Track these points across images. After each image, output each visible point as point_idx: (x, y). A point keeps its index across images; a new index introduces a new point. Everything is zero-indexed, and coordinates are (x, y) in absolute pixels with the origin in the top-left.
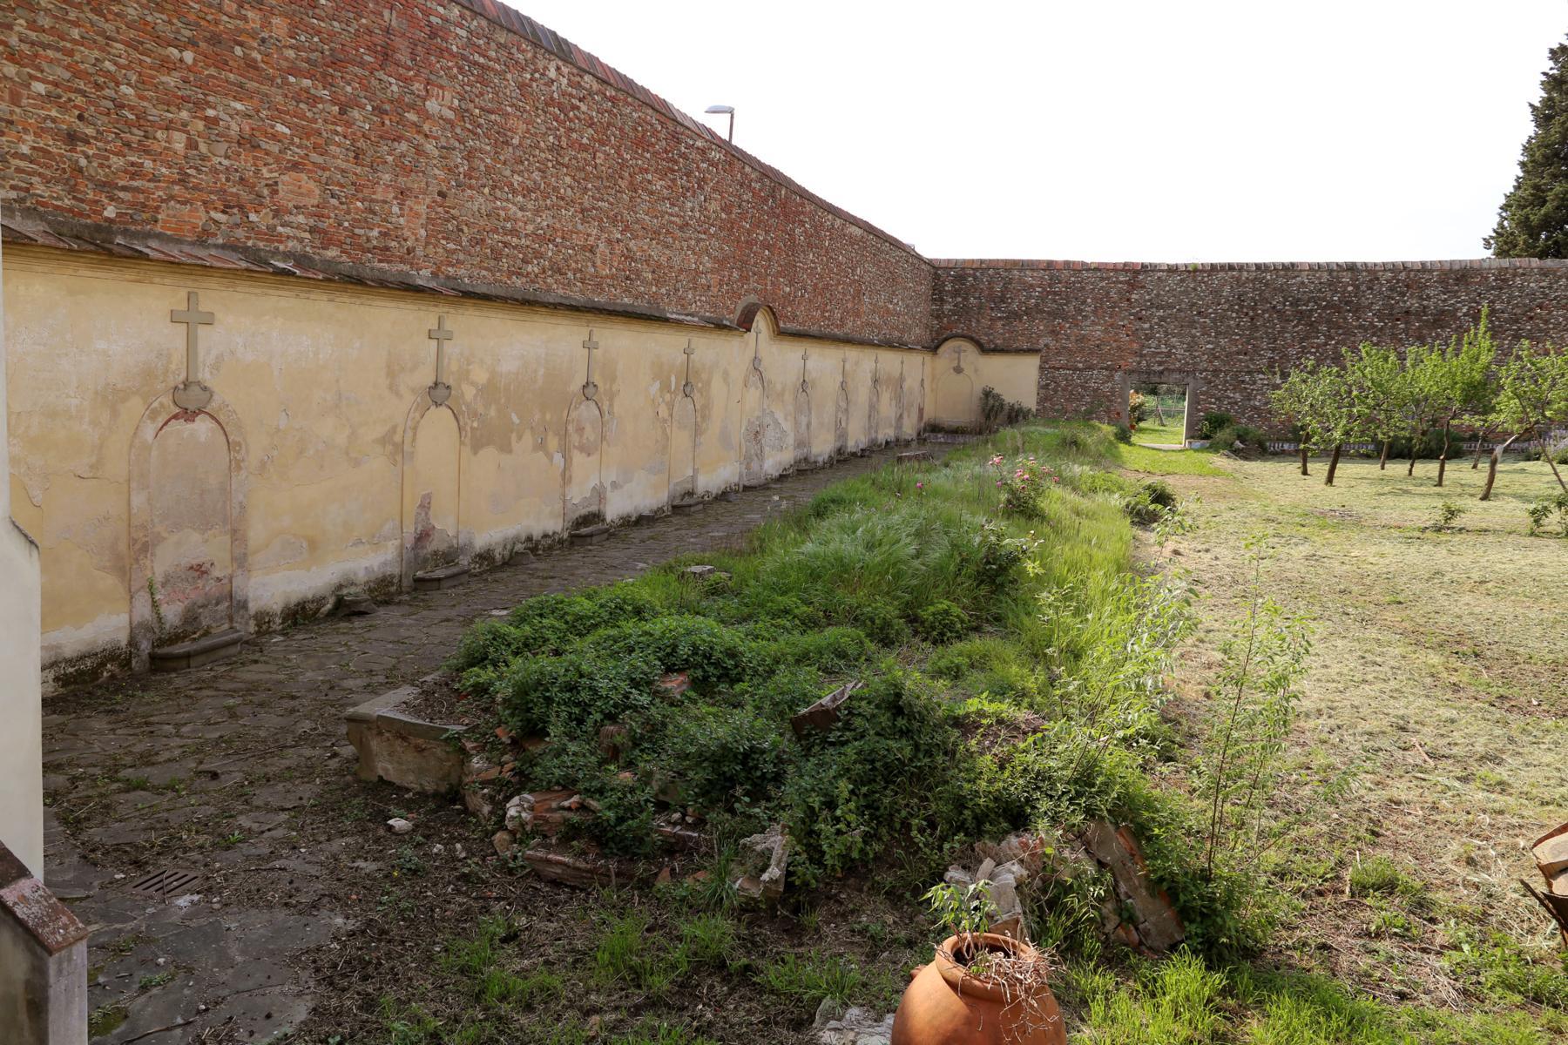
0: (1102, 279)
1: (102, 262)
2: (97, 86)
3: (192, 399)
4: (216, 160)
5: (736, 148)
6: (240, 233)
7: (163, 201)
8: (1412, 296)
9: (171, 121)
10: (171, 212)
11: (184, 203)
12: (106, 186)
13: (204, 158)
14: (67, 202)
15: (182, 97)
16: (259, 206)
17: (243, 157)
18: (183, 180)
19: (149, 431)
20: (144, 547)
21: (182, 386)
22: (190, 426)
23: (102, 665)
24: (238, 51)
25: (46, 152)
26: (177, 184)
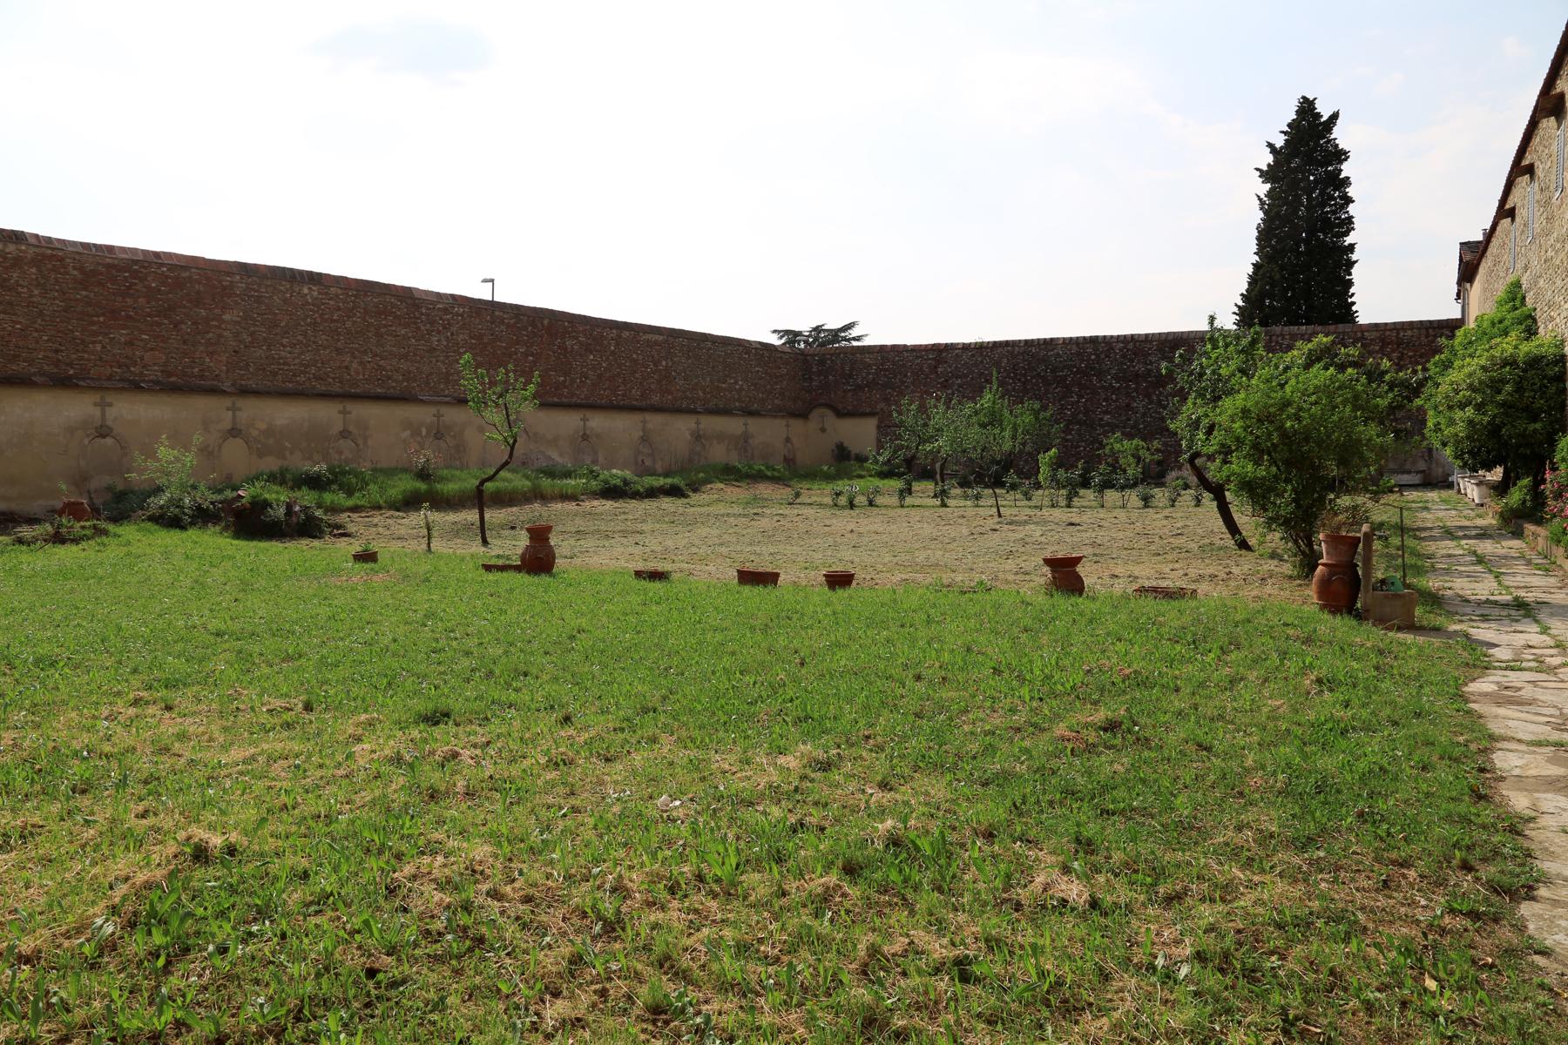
0: (917, 357)
5: (499, 303)
8: (1138, 363)
12: (71, 365)
14: (55, 370)
16: (135, 364)
18: (101, 359)
19: (86, 441)
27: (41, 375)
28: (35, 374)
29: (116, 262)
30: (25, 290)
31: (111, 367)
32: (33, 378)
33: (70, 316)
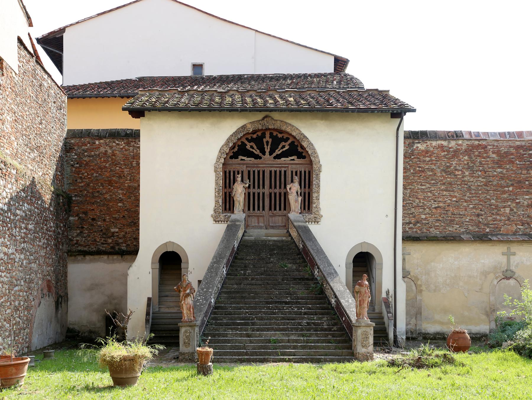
1: (482, 242)
3: (509, 274)
4: (519, 213)
6: (528, 230)
7: (502, 225)
9: (505, 206)
10: (505, 228)
11: (509, 225)
12: (487, 225)
13: (515, 213)
15: (508, 199)
17: (528, 210)
19: (495, 282)
20: (494, 311)
21: (505, 271)
22: (508, 281)
23: (482, 337)
24: (527, 183)
25: (472, 220)
26: (507, 221)
27: (468, 233)
28: (463, 233)
29: (523, 143)
30: (460, 173)
31: (516, 224)
32: (462, 236)
33: (488, 188)
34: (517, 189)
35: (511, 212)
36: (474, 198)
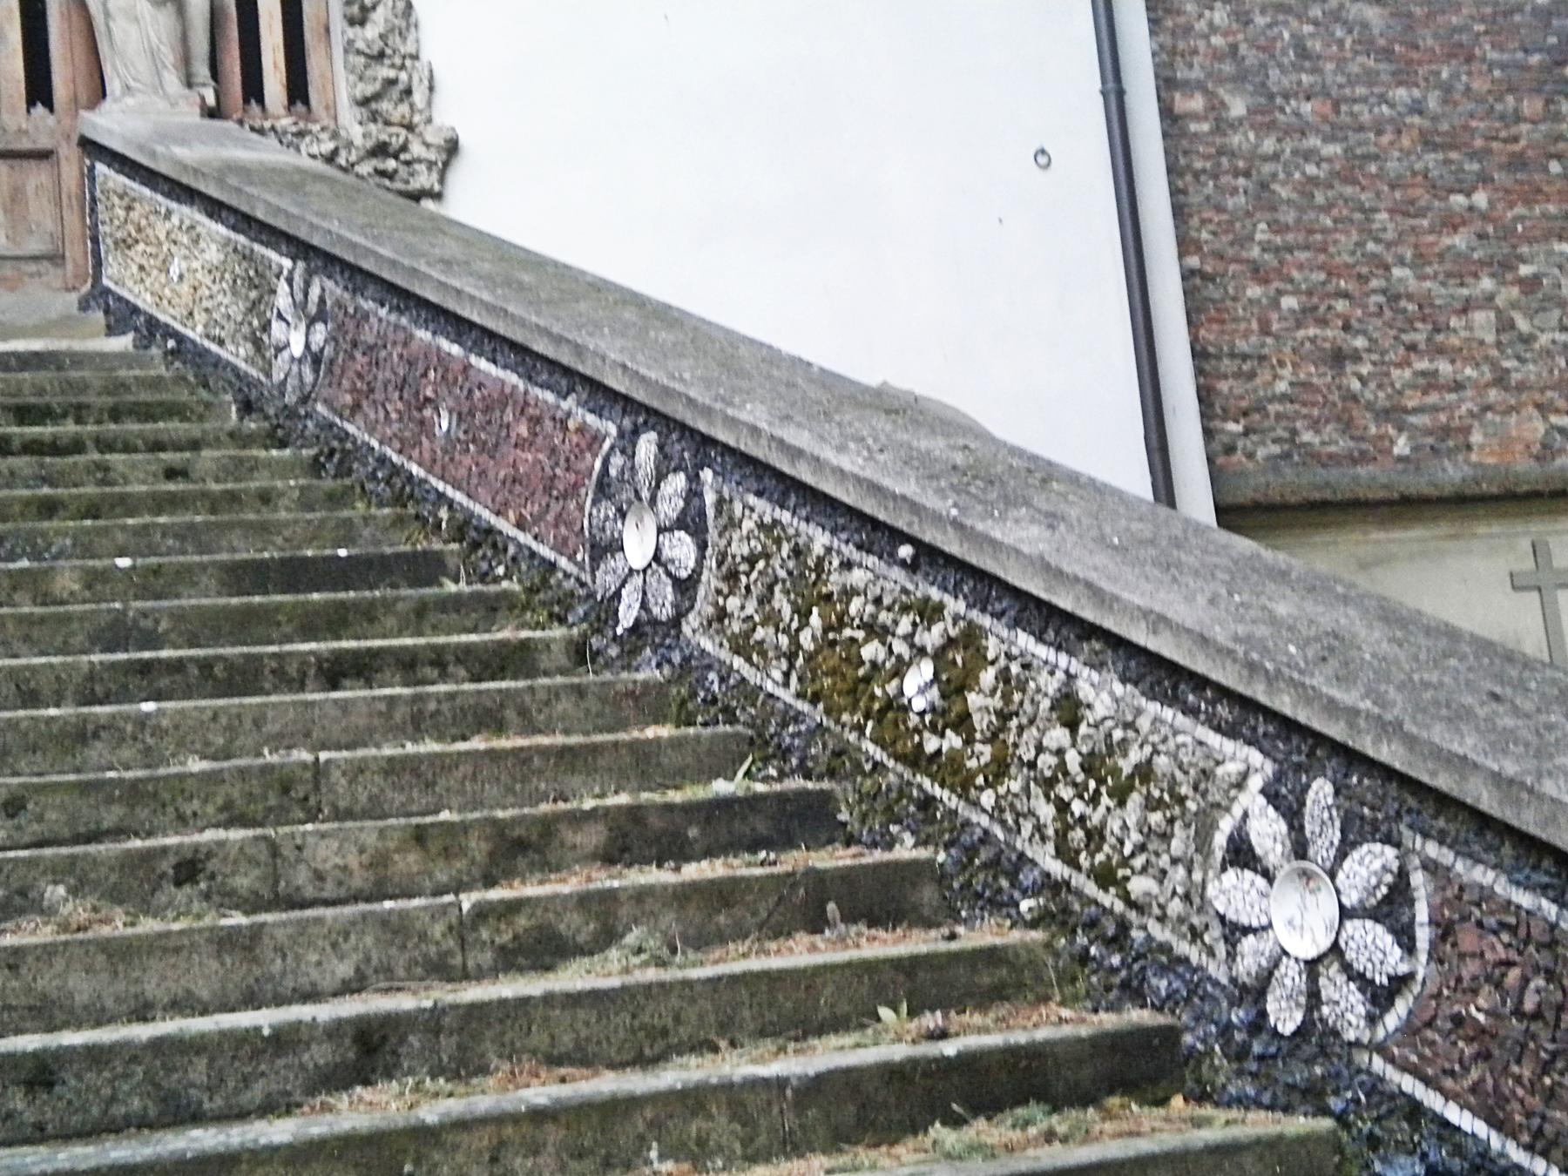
2: (1363, 279)
12: (1393, 413)
13: (1527, 340)
18: (1500, 379)
25: (1306, 385)
34: (1511, 205)
35: (1504, 338)
36: (1302, 256)
